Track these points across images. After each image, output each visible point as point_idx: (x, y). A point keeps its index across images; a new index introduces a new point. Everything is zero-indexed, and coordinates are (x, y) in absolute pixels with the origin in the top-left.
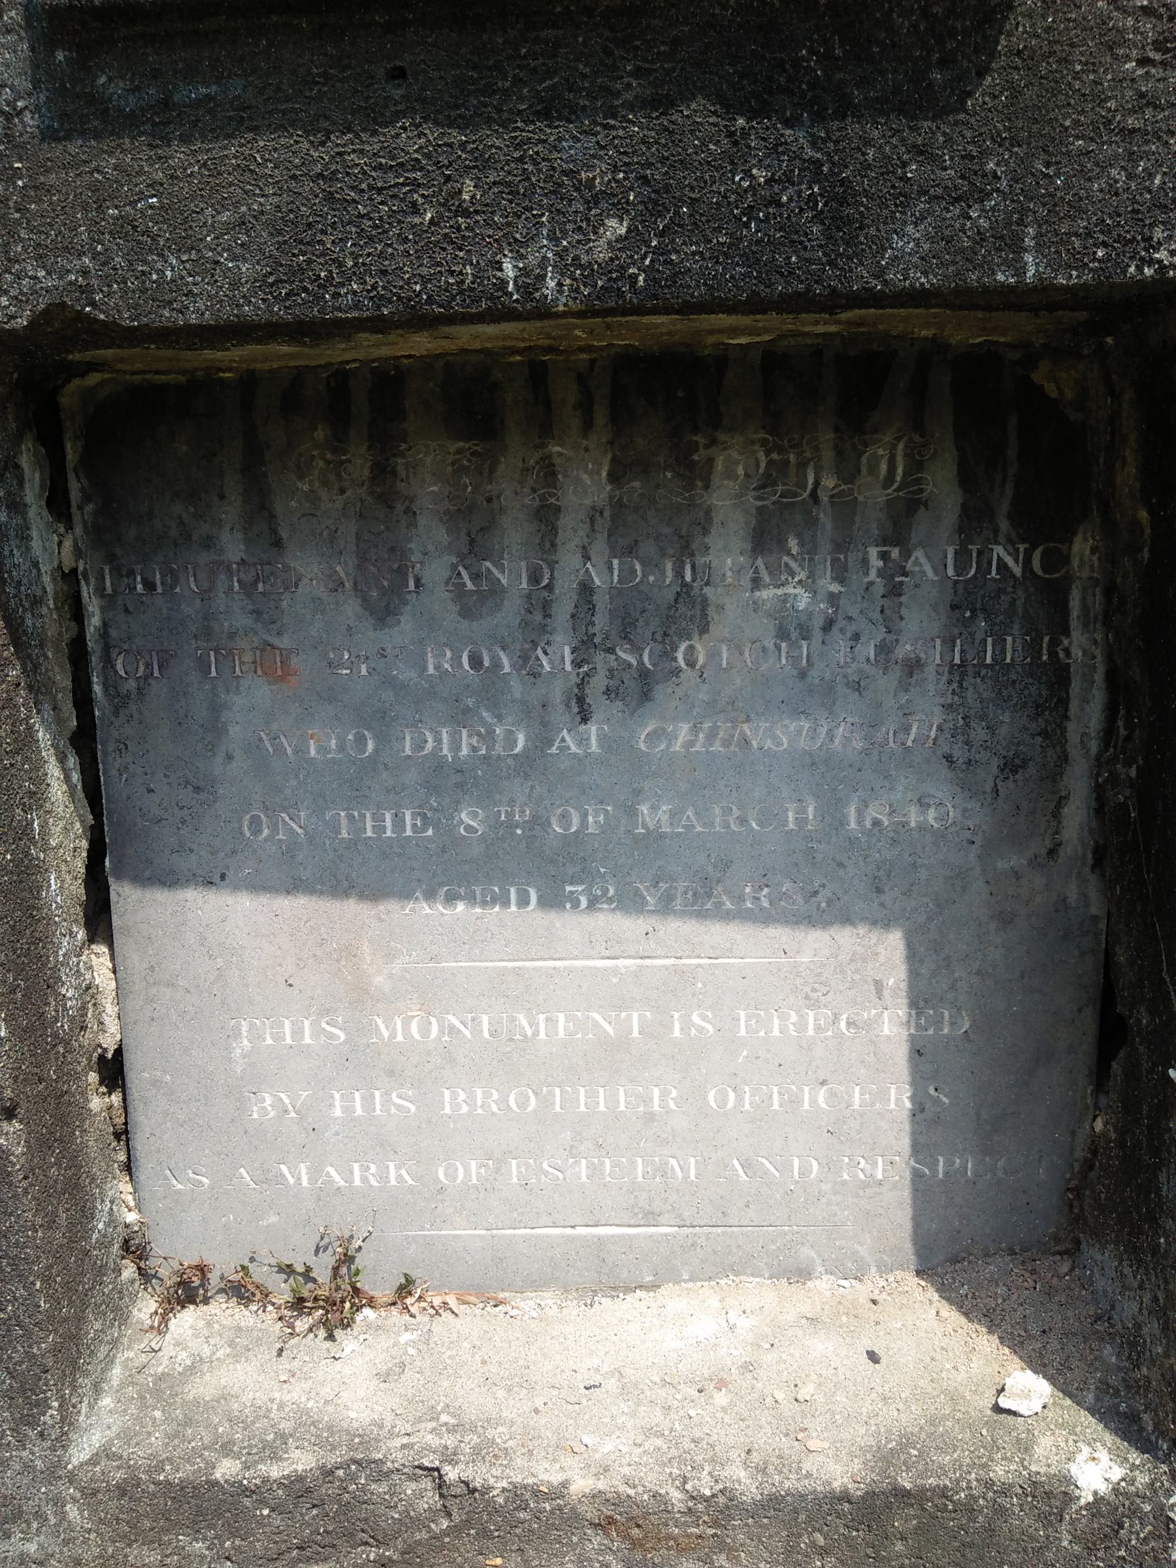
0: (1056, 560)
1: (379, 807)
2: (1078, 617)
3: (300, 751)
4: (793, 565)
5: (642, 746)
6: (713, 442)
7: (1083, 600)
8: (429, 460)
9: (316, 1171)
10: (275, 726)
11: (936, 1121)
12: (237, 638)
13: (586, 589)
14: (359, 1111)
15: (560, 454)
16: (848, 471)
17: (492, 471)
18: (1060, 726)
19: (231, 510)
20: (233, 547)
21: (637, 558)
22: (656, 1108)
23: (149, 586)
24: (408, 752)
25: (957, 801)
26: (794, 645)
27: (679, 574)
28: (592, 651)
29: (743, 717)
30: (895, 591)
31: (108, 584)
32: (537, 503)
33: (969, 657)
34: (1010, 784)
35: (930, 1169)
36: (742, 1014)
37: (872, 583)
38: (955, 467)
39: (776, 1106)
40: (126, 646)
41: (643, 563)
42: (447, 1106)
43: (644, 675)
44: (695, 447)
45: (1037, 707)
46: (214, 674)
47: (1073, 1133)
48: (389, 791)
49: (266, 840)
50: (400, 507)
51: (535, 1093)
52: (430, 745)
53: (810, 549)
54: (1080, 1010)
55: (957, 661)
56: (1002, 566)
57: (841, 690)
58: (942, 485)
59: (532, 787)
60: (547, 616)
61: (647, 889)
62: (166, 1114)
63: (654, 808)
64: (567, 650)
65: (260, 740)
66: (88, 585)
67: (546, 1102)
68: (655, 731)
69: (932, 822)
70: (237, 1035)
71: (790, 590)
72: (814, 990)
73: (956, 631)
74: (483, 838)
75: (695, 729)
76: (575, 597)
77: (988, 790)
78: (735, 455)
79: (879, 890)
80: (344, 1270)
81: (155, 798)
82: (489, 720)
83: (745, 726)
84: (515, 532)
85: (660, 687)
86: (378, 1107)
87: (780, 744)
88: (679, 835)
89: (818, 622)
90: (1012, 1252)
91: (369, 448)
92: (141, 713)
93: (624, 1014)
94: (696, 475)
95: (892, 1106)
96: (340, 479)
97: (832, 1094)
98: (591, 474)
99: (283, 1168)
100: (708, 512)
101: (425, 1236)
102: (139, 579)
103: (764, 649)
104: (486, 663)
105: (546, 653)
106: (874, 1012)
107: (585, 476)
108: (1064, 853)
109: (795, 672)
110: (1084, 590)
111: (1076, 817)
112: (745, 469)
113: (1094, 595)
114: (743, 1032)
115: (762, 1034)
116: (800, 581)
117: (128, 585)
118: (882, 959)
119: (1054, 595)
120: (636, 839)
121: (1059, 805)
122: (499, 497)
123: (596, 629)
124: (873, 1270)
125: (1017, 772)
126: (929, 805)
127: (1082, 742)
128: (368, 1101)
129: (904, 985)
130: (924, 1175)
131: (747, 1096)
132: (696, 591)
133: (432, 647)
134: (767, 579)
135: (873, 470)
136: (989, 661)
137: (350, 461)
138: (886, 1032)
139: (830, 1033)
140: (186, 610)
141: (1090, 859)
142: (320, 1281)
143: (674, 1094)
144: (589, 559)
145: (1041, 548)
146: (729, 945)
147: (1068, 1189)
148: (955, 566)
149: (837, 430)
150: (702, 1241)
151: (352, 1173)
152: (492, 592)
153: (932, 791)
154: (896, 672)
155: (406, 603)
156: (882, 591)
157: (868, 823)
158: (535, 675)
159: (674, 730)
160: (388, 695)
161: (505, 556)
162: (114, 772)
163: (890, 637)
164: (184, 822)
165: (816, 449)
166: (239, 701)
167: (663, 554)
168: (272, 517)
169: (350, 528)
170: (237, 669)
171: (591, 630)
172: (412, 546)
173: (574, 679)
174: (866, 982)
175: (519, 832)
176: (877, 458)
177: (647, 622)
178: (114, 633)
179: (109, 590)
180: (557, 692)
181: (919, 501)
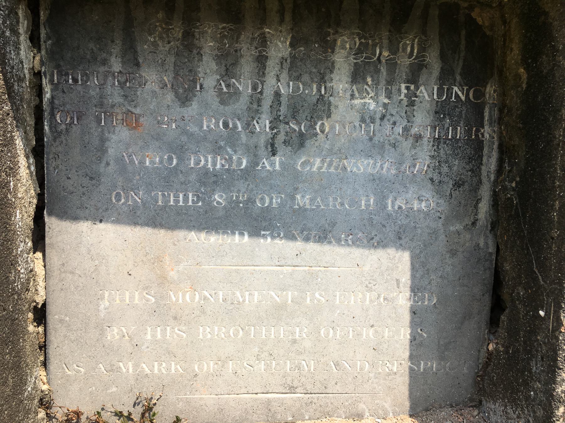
0: (479, 95)
1: (177, 191)
2: (488, 120)
3: (142, 162)
4: (368, 89)
5: (299, 168)
6: (337, 32)
7: (490, 113)
8: (210, 31)
9: (136, 366)
10: (130, 150)
11: (421, 345)
12: (115, 108)
13: (277, 94)
14: (159, 337)
15: (269, 33)
16: (394, 51)
17: (238, 38)
18: (478, 167)
19: (116, 49)
20: (116, 65)
21: (301, 82)
22: (297, 337)
23: (75, 81)
24: (192, 165)
25: (435, 199)
26: (367, 125)
27: (319, 90)
28: (279, 123)
29: (344, 157)
30: (411, 104)
31: (56, 78)
32: (258, 54)
33: (442, 135)
34: (457, 192)
35: (417, 367)
36: (338, 294)
37: (402, 100)
38: (439, 51)
39: (351, 337)
40: (61, 109)
41: (303, 84)
42: (201, 335)
43: (301, 135)
44: (328, 34)
45: (470, 158)
46: (103, 124)
47: (479, 351)
48: (182, 183)
49: (123, 204)
50: (195, 51)
51: (242, 329)
52: (202, 163)
53: (376, 83)
54: (483, 295)
55: (437, 136)
56: (457, 96)
57: (387, 147)
58: (433, 59)
59: (249, 185)
60: (259, 106)
61: (298, 234)
62: (65, 336)
63: (303, 197)
64: (267, 122)
65: (123, 156)
66: (46, 78)
67: (247, 333)
68: (305, 161)
69: (424, 208)
70: (102, 298)
71: (367, 100)
72: (370, 283)
73: (437, 123)
74: (225, 208)
75: (323, 161)
76: (272, 98)
77: (448, 195)
78: (346, 39)
79: (400, 238)
80: (147, 415)
81: (71, 182)
82: (230, 152)
83: (345, 161)
84: (247, 67)
85: (308, 141)
86: (168, 334)
87: (359, 170)
88: (313, 210)
89: (378, 116)
90: (452, 406)
91: (183, 23)
92: (67, 140)
93: (285, 292)
94: (329, 47)
95: (402, 338)
96: (168, 37)
97: (376, 332)
98: (282, 42)
99: (121, 364)
100: (333, 63)
101: (187, 398)
102: (70, 77)
103: (355, 126)
104: (231, 126)
105: (258, 123)
106: (395, 294)
107: (279, 43)
108: (480, 223)
109: (368, 138)
110: (490, 109)
111: (484, 207)
112: (350, 45)
113: (495, 111)
114: (338, 302)
115: (346, 303)
116: (371, 97)
117: (65, 80)
118: (400, 269)
119: (477, 109)
120: (294, 211)
121: (477, 203)
122: (240, 50)
123: (281, 113)
124: (391, 414)
125: (460, 187)
126: (422, 201)
127: (487, 175)
128: (164, 331)
129: (409, 282)
130: (414, 370)
131: (338, 332)
132: (326, 99)
133: (206, 116)
134: (357, 95)
135: (404, 50)
136: (450, 137)
137: (173, 29)
138: (400, 303)
139: (376, 303)
140: (92, 93)
141: (489, 228)
142: (135, 420)
143: (306, 330)
144: (280, 81)
145: (473, 89)
146: (333, 261)
147: (478, 376)
148: (437, 94)
149: (390, 31)
150: (315, 401)
151: (153, 367)
152: (235, 93)
153: (424, 194)
154: (411, 140)
155: (195, 96)
156: (406, 104)
157: (396, 207)
158: (252, 133)
159: (314, 161)
160: (184, 138)
161: (242, 77)
162: (51, 169)
163: (408, 124)
164: (84, 194)
165: (381, 39)
166: (114, 138)
167: (313, 82)
168: (136, 52)
169: (171, 59)
170: (114, 122)
171: (279, 113)
172: (200, 70)
173: (270, 136)
174: (393, 280)
175: (241, 205)
176: (405, 45)
177: (304, 111)
178: (56, 102)
179: (56, 81)
180: (262, 141)
181: (423, 65)
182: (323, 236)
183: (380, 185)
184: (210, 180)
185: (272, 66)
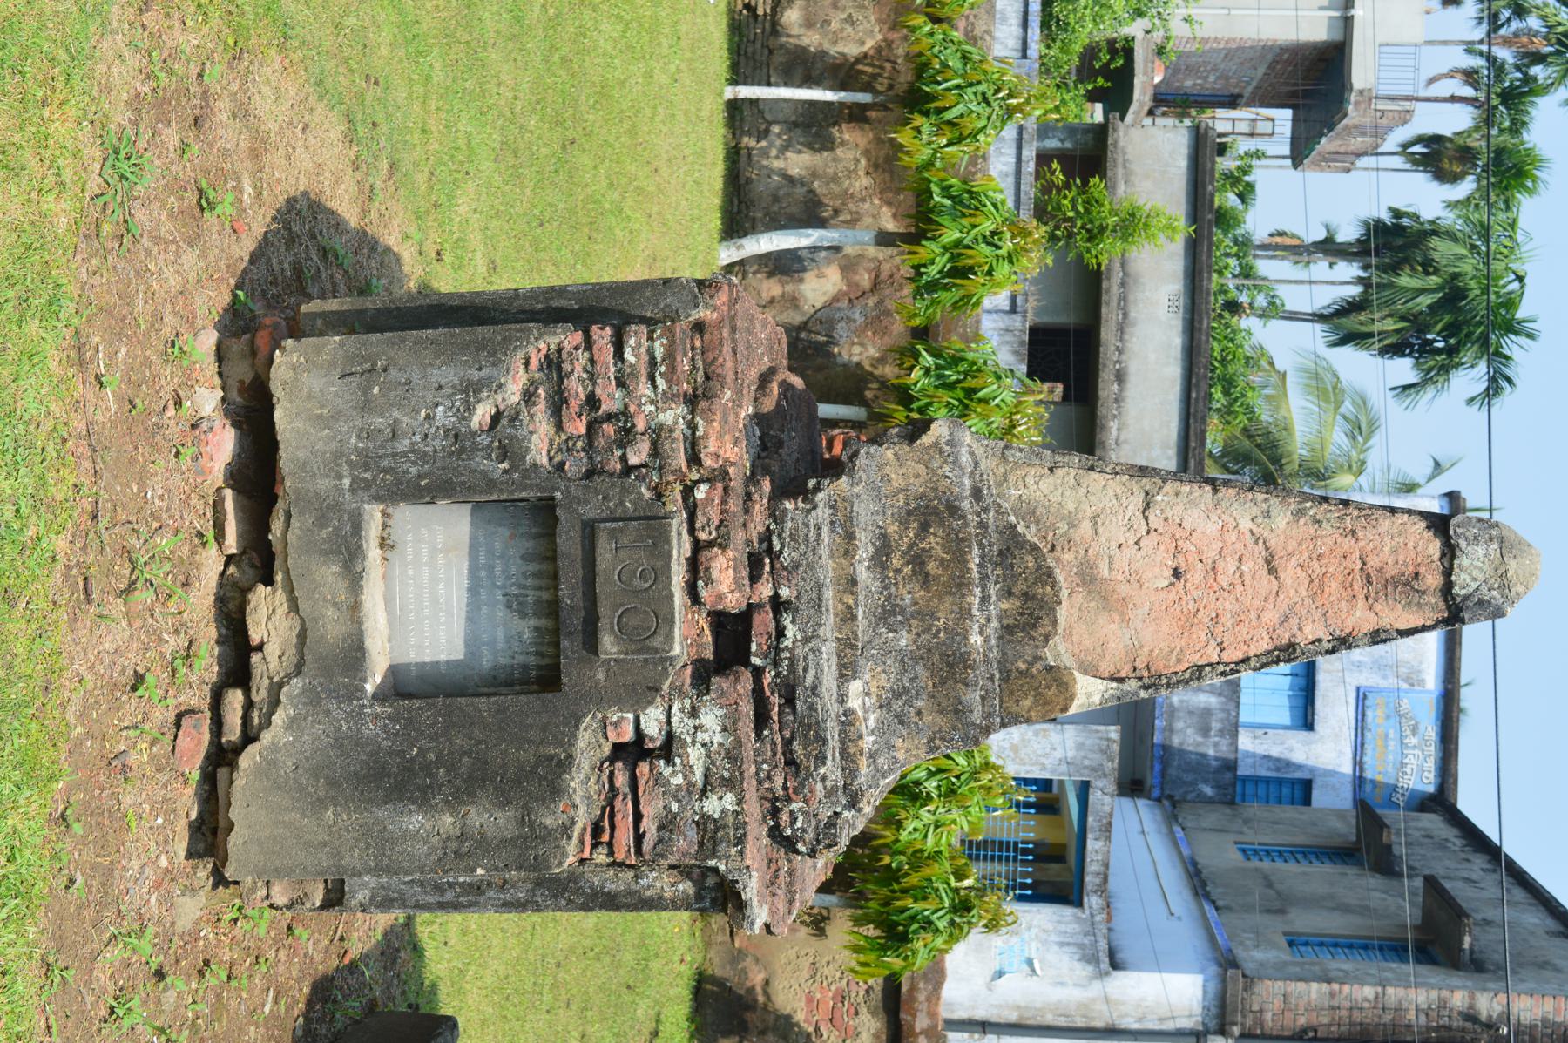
58: (546, 661)
84: (537, 582)
94: (548, 616)
119: (526, 683)
183: (493, 642)
184: (490, 569)
185: (538, 593)
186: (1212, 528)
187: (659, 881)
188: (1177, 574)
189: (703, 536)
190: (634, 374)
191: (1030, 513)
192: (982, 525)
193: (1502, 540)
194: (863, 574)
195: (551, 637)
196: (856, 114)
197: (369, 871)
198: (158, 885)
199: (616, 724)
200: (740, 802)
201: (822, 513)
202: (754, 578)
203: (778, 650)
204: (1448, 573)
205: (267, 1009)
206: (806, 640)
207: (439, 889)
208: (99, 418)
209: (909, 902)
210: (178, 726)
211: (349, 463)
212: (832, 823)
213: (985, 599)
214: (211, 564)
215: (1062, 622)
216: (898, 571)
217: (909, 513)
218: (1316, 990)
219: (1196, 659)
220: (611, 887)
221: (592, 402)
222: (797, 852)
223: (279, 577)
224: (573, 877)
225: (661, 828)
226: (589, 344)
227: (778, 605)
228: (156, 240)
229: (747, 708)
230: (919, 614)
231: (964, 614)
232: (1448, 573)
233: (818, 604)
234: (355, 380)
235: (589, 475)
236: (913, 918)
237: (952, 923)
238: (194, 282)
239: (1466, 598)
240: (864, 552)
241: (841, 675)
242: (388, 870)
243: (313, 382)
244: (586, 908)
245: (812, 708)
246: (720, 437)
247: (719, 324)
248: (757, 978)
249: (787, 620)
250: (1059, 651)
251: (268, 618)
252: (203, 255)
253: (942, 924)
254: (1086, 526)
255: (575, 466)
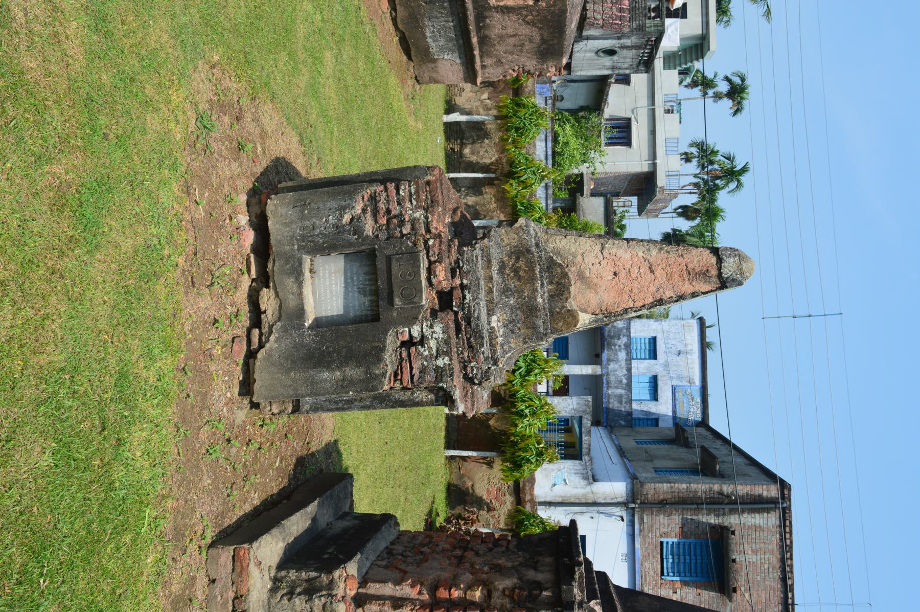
182: (345, 298)
183: (354, 306)
186: (628, 256)
187: (421, 395)
188: (615, 274)
189: (432, 259)
190: (404, 199)
191: (558, 253)
192: (540, 257)
193: (739, 256)
194: (495, 276)
195: (375, 304)
196: (489, 182)
197: (308, 395)
198: (227, 404)
199: (402, 333)
200: (451, 360)
201: (478, 252)
202: (453, 277)
203: (463, 304)
204: (719, 269)
205: (277, 464)
206: (474, 300)
207: (336, 403)
208: (197, 216)
209: (521, 453)
210: (233, 342)
211: (297, 239)
212: (487, 371)
213: (542, 285)
214: (246, 283)
215: (572, 293)
216: (508, 275)
217: (512, 253)
218: (666, 486)
219: (624, 306)
220: (402, 398)
221: (388, 211)
222: (475, 384)
223: (271, 285)
224: (388, 395)
225: (420, 372)
226: (386, 189)
227: (463, 287)
228: (221, 156)
229: (452, 325)
230: (517, 291)
231: (535, 290)
232: (719, 269)
233: (478, 286)
234: (299, 208)
235: (388, 239)
236: (523, 459)
237: (537, 460)
238: (237, 177)
239: (727, 278)
240: (495, 267)
241: (488, 314)
242: (315, 394)
243: (282, 210)
244: (393, 407)
245: (477, 325)
246: (438, 222)
247: (436, 181)
248: (469, 484)
249: (466, 292)
250: (572, 304)
251: (268, 301)
252: (240, 165)
253: (533, 461)
254: (579, 258)
255: (382, 236)
